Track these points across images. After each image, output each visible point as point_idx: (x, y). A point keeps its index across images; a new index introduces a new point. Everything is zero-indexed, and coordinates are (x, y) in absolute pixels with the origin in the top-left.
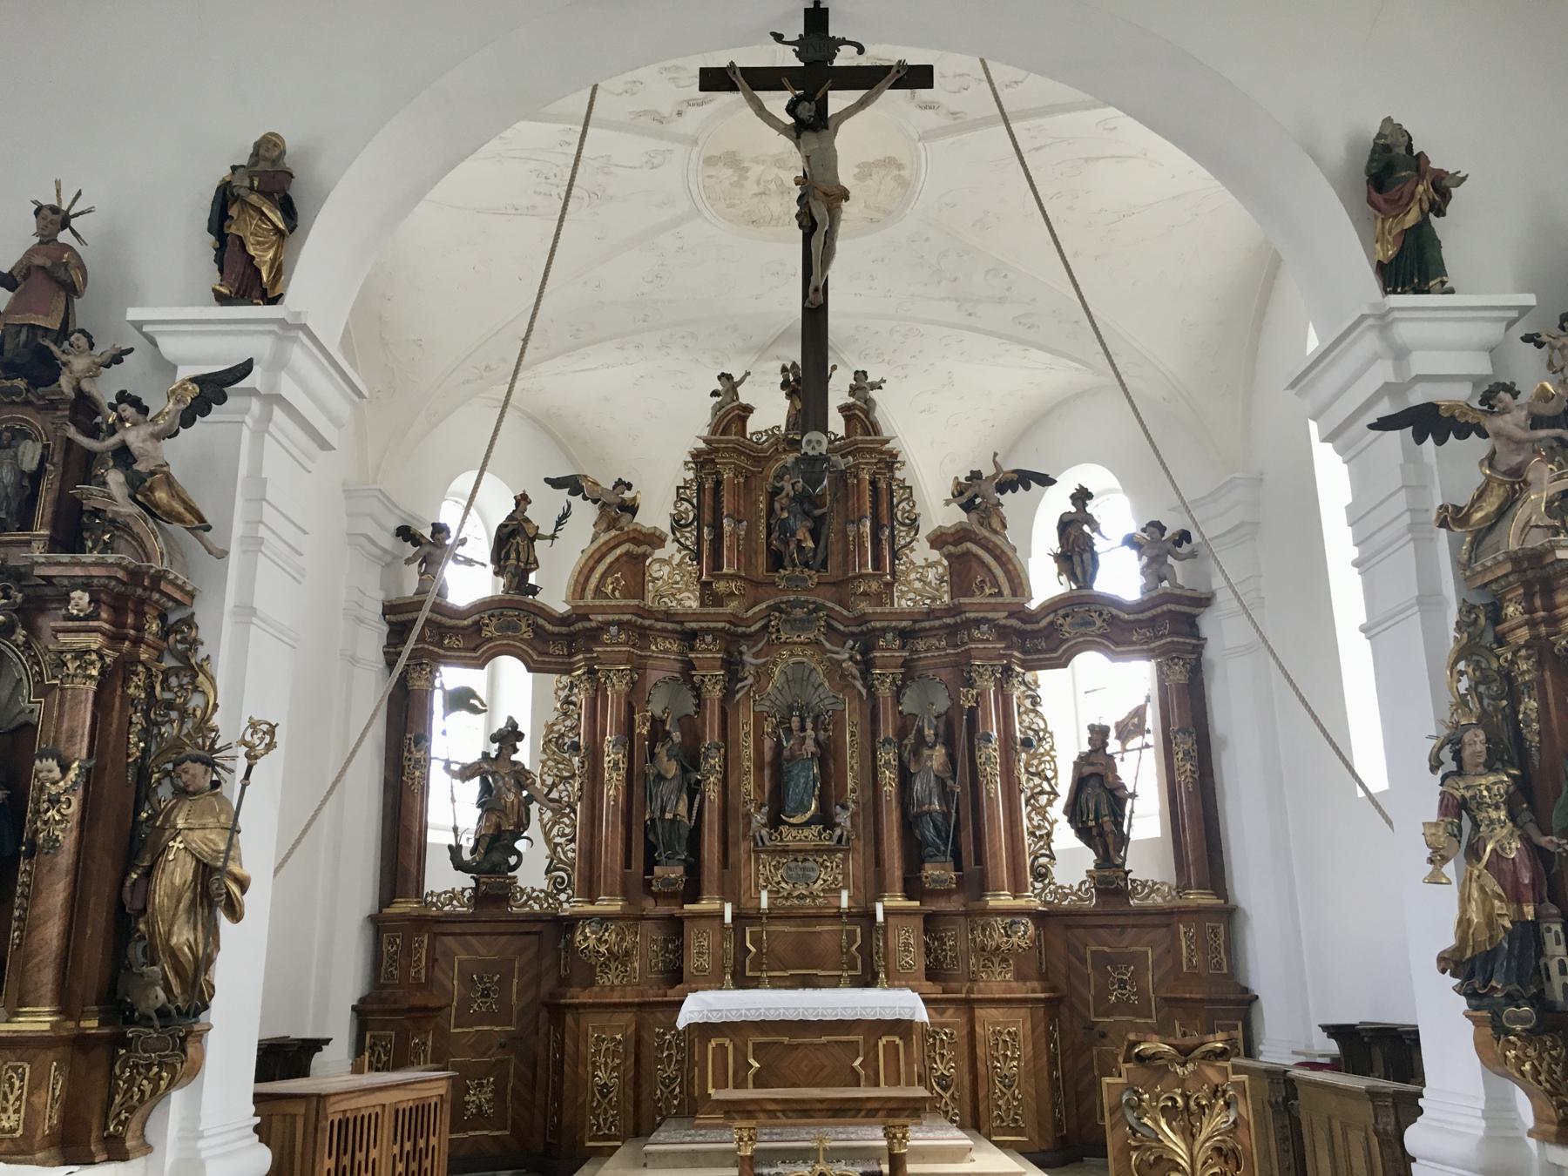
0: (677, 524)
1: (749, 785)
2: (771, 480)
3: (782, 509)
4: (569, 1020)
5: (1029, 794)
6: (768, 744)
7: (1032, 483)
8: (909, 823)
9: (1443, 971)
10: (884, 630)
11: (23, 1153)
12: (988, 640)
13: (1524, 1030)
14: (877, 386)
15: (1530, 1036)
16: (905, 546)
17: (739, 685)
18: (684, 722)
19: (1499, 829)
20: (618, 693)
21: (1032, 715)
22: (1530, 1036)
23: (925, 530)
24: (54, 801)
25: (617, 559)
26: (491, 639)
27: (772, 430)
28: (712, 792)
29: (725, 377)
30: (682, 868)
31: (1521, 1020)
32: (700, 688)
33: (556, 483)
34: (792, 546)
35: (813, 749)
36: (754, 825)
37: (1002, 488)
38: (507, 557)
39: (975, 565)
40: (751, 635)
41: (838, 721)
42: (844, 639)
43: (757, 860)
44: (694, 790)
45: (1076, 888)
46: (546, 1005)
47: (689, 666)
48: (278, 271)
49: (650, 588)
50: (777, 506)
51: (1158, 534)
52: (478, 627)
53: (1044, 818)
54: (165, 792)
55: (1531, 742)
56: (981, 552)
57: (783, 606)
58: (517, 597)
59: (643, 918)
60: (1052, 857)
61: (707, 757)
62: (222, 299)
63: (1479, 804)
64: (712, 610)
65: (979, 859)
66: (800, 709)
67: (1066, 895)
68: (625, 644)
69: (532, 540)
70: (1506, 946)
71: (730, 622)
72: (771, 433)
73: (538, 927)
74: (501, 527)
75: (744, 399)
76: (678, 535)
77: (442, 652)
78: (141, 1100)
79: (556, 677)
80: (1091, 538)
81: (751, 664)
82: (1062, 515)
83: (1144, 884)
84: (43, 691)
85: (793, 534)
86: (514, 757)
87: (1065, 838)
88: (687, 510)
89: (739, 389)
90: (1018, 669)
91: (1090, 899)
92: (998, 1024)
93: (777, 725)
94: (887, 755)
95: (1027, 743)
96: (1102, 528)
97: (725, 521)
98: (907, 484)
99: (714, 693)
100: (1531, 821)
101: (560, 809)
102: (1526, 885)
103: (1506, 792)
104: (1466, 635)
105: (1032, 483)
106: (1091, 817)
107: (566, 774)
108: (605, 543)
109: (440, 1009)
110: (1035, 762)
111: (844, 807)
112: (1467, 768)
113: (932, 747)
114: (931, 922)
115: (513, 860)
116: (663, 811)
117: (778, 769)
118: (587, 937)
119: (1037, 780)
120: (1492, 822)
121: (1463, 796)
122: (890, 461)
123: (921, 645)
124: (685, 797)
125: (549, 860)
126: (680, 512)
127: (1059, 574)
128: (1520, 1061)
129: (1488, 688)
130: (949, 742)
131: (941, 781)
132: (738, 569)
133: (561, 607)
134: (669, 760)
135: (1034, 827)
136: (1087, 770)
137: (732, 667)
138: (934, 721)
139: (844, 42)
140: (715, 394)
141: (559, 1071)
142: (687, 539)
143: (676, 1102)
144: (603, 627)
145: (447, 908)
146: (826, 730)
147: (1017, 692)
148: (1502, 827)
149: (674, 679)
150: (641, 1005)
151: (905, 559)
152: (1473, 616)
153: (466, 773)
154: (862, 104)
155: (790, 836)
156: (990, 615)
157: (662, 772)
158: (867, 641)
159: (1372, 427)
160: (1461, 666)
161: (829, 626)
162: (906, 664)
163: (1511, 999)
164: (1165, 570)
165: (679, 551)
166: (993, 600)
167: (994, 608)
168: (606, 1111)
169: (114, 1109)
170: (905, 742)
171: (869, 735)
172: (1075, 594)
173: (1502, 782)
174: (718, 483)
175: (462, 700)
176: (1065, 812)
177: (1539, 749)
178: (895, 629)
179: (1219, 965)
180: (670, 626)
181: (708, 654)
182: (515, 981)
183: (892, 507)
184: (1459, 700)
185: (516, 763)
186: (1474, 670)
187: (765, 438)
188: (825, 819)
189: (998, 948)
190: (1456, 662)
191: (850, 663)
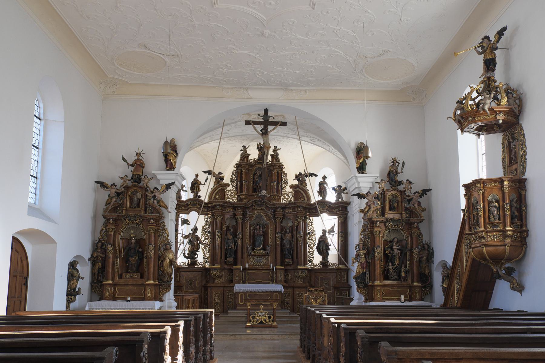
0: (232, 181)
1: (247, 241)
2: (254, 171)
3: (256, 178)
4: (209, 289)
5: (309, 244)
6: (252, 232)
7: (313, 176)
8: (282, 250)
9: (353, 279)
10: (279, 207)
11: (151, 299)
12: (301, 211)
14: (280, 149)
16: (285, 187)
17: (246, 219)
18: (233, 226)
20: (219, 221)
21: (311, 227)
23: (289, 184)
24: (151, 251)
25: (219, 190)
26: (190, 208)
27: (254, 159)
28: (240, 243)
29: (244, 147)
30: (233, 259)
31: (361, 285)
32: (236, 220)
33: (205, 172)
34: (258, 187)
35: (262, 233)
36: (249, 250)
37: (306, 176)
38: (194, 189)
39: (300, 194)
40: (249, 207)
41: (268, 227)
42: (270, 209)
43: (249, 257)
44: (236, 242)
45: (318, 264)
46: (203, 286)
47: (234, 215)
48: (175, 163)
49: (226, 197)
50: (255, 177)
51: (339, 188)
52: (188, 205)
53: (312, 249)
54: (162, 249)
56: (301, 191)
57: (256, 201)
58: (196, 198)
59: (224, 269)
60: (313, 258)
61: (238, 235)
62: (168, 170)
64: (240, 202)
65: (297, 258)
66: (259, 224)
67: (315, 266)
68: (220, 210)
69: (199, 185)
70: (361, 275)
71: (244, 205)
72: (254, 160)
73: (201, 270)
74: (192, 182)
75: (248, 153)
76: (232, 183)
77: (180, 211)
78: (164, 293)
79: (204, 216)
80: (325, 187)
81: (249, 214)
82: (320, 182)
83: (332, 264)
84: (146, 234)
85: (259, 184)
86: (196, 234)
87: (316, 254)
88: (234, 178)
89: (247, 150)
90: (308, 217)
91: (320, 267)
92: (299, 292)
93: (254, 228)
94: (278, 235)
95: (309, 233)
96: (328, 186)
97: (243, 182)
98: (285, 172)
99: (240, 220)
101: (206, 245)
105: (313, 176)
106: (321, 250)
107: (207, 238)
108: (217, 187)
109: (182, 286)
110: (311, 237)
111: (269, 246)
113: (288, 234)
114: (286, 271)
115: (196, 256)
116: (229, 247)
117: (253, 238)
118: (213, 273)
119: (311, 241)
120: (362, 257)
122: (281, 167)
123: (287, 211)
124: (234, 243)
125: (203, 256)
126: (233, 178)
127: (319, 195)
128: (361, 291)
130: (292, 232)
131: (290, 241)
132: (246, 192)
133: (206, 201)
134: (230, 235)
135: (310, 251)
136: (321, 240)
137: (244, 215)
138: (289, 228)
139: (271, 116)
140: (241, 150)
141: (207, 299)
142: (234, 184)
143: (231, 306)
144: (215, 206)
145: (182, 266)
146: (265, 229)
147: (308, 221)
149: (232, 217)
150: (224, 287)
151: (284, 190)
153: (186, 237)
154: (274, 129)
155: (256, 252)
156: (302, 205)
157: (229, 238)
158: (275, 210)
159: (352, 195)
160: (362, 234)
161: (266, 206)
162: (284, 215)
163: (361, 283)
164: (340, 196)
165: (232, 187)
166: (303, 202)
167: (303, 204)
168: (217, 308)
169: (160, 295)
170: (282, 232)
171: (274, 230)
172: (322, 200)
174: (242, 172)
175: (185, 222)
176: (316, 248)
178: (281, 207)
179: (345, 280)
180: (230, 205)
181: (239, 212)
182: (197, 282)
183: (282, 178)
185: (196, 235)
187: (253, 161)
188: (264, 249)
189: (300, 276)
190: (361, 233)
191: (271, 215)
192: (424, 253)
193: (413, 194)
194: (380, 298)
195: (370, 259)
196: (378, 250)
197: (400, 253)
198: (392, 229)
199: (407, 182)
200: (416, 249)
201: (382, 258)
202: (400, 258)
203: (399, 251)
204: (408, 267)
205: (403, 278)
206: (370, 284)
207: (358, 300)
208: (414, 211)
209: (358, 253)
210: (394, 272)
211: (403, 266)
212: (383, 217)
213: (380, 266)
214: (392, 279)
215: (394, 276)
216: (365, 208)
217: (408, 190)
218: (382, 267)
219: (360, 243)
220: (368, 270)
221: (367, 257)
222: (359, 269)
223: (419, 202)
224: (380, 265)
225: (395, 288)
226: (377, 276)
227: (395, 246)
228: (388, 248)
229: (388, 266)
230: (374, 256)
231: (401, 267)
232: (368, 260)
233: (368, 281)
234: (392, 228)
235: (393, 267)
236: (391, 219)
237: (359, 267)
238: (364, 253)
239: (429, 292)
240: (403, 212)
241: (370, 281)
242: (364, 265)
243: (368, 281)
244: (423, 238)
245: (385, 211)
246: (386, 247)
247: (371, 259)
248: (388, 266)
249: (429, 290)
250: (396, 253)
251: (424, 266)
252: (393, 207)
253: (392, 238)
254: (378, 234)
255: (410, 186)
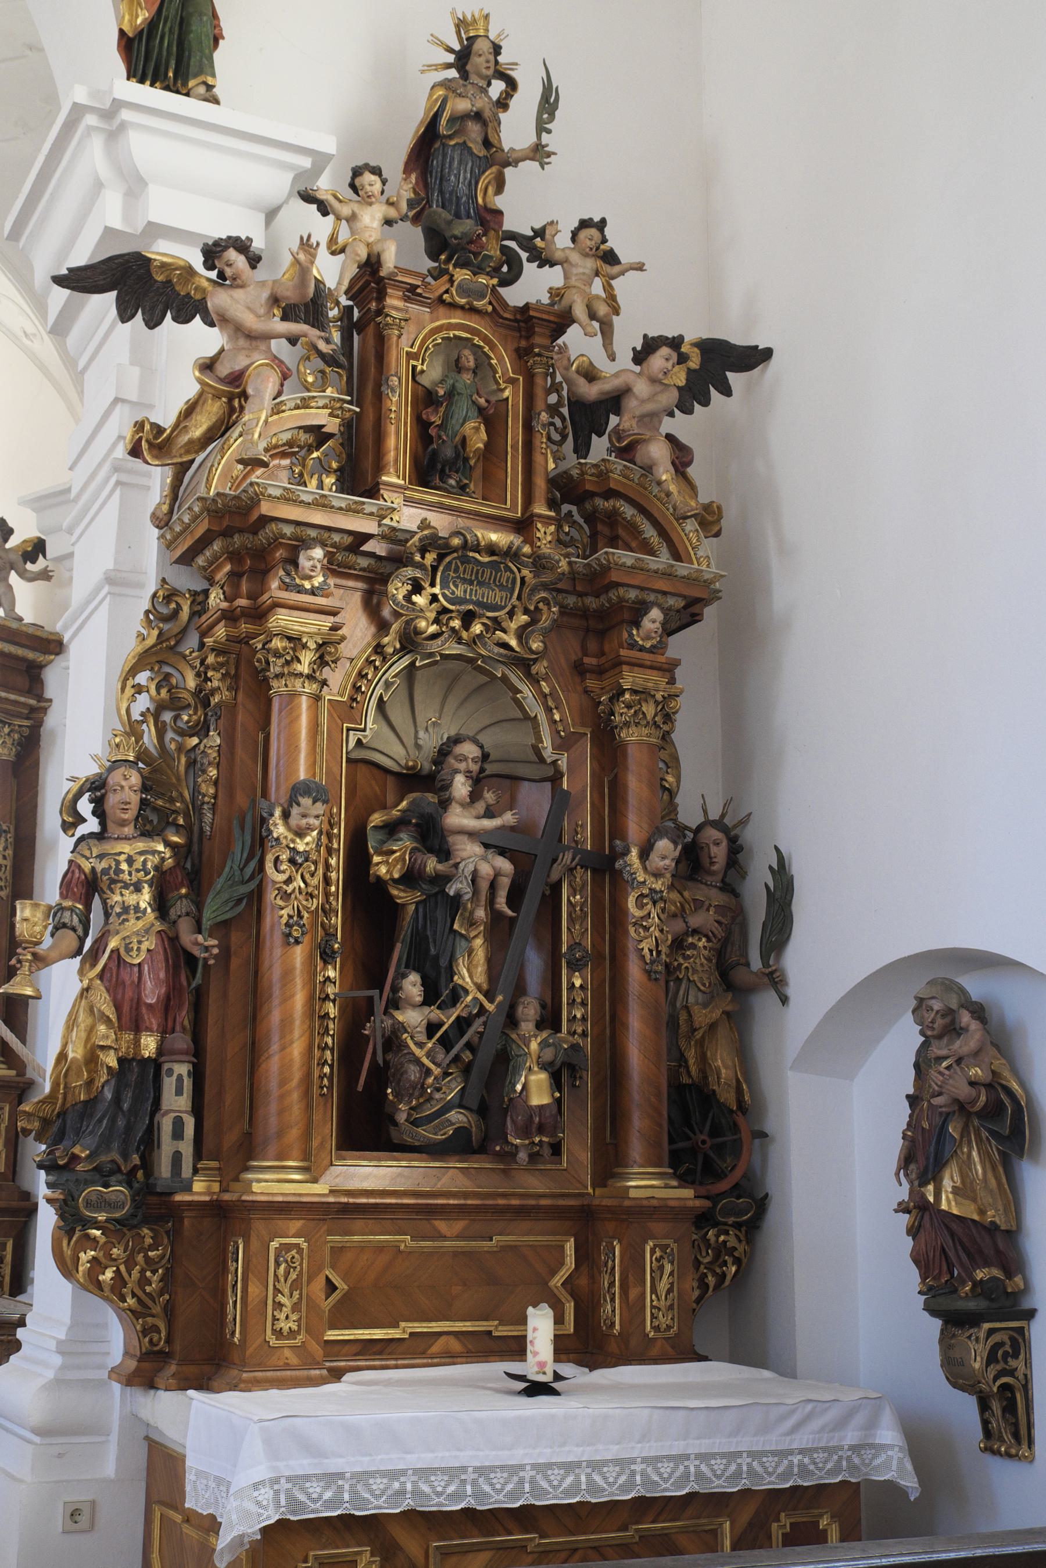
13: (107, 1221)
15: (118, 1228)
19: (133, 921)
22: (118, 1228)
31: (103, 1204)
55: (204, 796)
63: (113, 881)
70: (108, 1095)
100: (187, 914)
102: (150, 1006)
103: (156, 868)
104: (156, 632)
112: (113, 830)
120: (126, 909)
121: (93, 868)
129: (176, 718)
148: (138, 918)
152: (173, 606)
160: (143, 678)
163: (103, 1175)
173: (154, 852)
177: (214, 808)
184: (128, 729)
186: (158, 688)
190: (133, 671)
192: (698, 905)
193: (624, 359)
194: (298, 1341)
195: (206, 924)
196: (300, 833)
197: (505, 882)
198: (435, 646)
199: (584, 234)
200: (663, 845)
201: (337, 921)
202: (495, 916)
203: (505, 865)
204: (572, 1019)
205: (525, 1131)
206: (198, 1186)
207: (57, 1360)
208: (628, 511)
209: (87, 866)
210: (446, 1074)
211: (529, 1010)
212: (370, 505)
213: (311, 999)
214: (427, 1133)
215: (447, 1108)
216: (190, 410)
217: (592, 316)
218: (332, 1010)
219: (115, 764)
220: (181, 1041)
221: (180, 908)
222: (91, 1030)
223: (670, 437)
224: (317, 998)
225: (442, 1226)
226: (273, 1107)
227: (463, 805)
228: (391, 829)
229: (386, 1012)
230: (257, 896)
231: (512, 1021)
232: (189, 938)
233: (177, 1157)
234: (434, 636)
235: (434, 1014)
236: (432, 542)
237: (91, 1009)
238: (152, 861)
239: (737, 1261)
240: (540, 509)
241: (198, 1155)
242: (149, 984)
243: (177, 1157)
244: (678, 781)
245: (379, 468)
246: (377, 819)
247: (222, 928)
248: (394, 1003)
249: (732, 1242)
250: (475, 874)
251: (703, 1017)
252: (449, 452)
253: (431, 741)
254: (304, 668)
255: (608, 288)
